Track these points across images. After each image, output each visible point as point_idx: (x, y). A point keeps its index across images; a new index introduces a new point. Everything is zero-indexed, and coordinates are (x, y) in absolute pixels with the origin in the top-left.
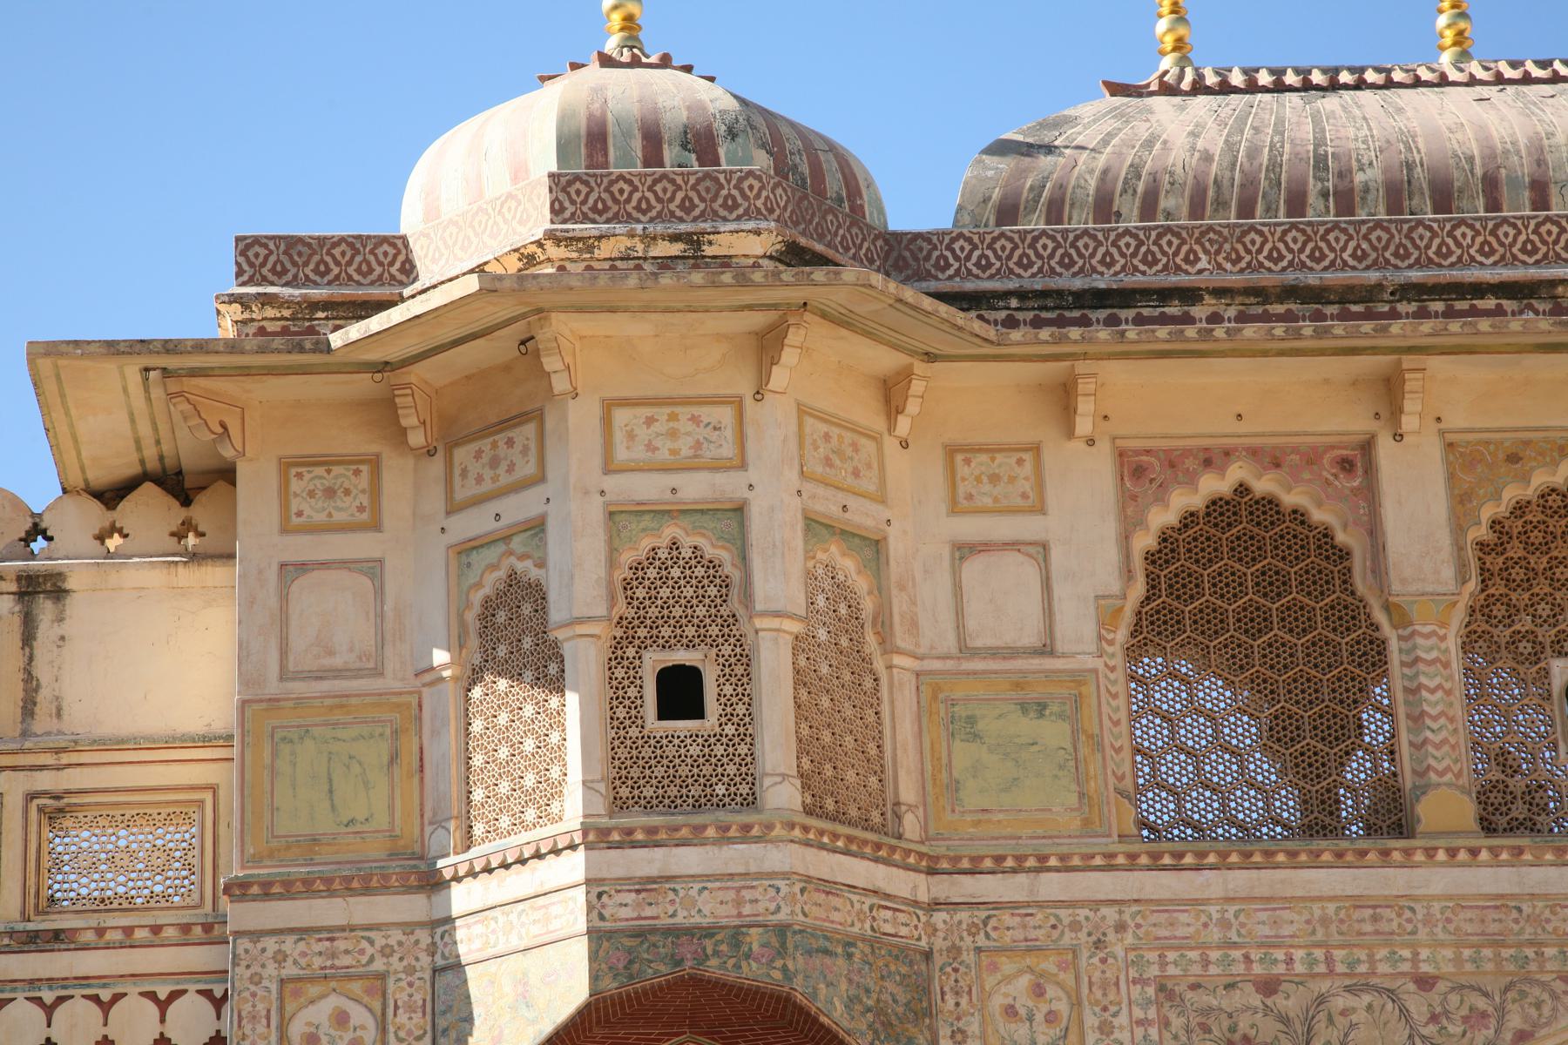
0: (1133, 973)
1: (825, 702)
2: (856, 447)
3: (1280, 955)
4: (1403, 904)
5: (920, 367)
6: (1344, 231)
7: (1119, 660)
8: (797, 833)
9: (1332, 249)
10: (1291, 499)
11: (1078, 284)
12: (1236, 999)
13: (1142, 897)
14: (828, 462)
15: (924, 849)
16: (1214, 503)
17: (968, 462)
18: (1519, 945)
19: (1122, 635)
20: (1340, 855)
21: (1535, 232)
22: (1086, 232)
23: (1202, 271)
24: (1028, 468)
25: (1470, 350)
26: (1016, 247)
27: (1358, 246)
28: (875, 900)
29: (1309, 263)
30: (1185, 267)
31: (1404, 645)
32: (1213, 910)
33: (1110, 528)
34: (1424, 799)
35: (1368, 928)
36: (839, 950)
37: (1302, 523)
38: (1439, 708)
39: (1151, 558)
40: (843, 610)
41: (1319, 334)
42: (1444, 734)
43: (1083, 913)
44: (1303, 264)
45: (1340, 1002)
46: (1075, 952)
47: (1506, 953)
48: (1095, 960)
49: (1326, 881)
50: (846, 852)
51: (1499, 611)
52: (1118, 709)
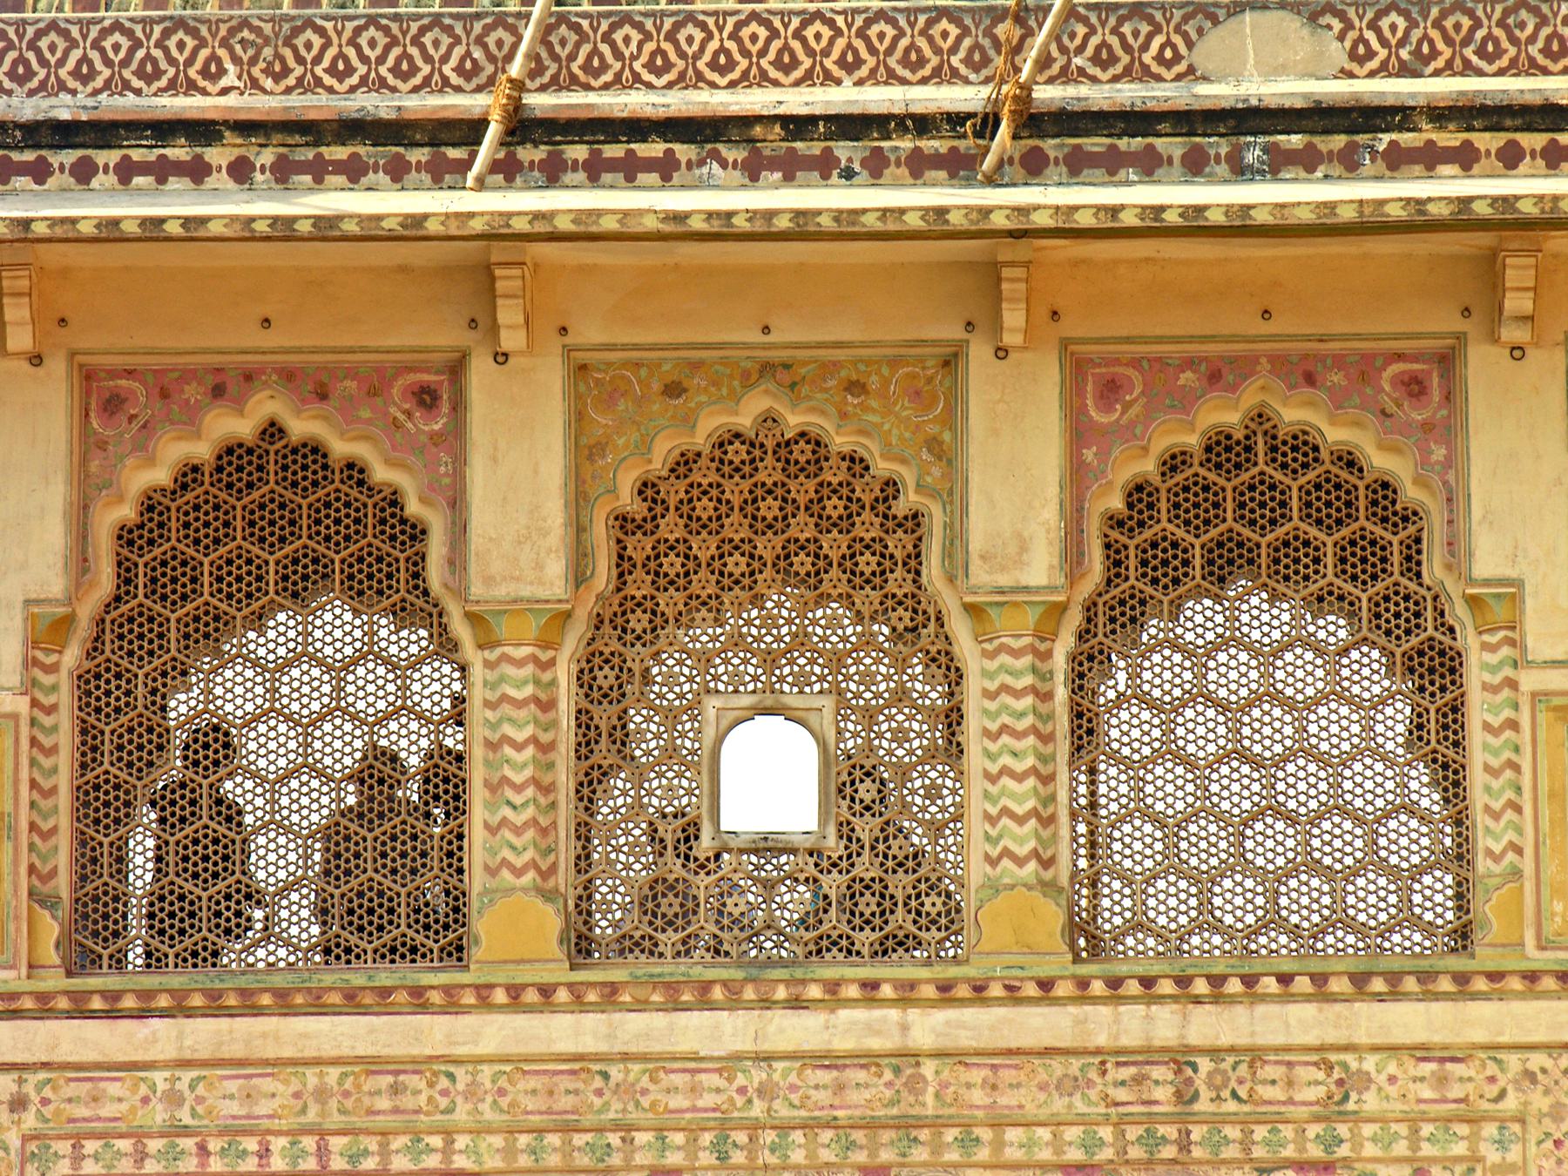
3: (251, 1144)
6: (449, 30)
9: (428, 59)
13: (56, 1058)
16: (230, 451)
18: (600, 1130)
19: (72, 657)
21: (734, 36)
22: (53, 26)
27: (468, 54)
29: (391, 80)
30: (202, 83)
31: (491, 676)
32: (159, 1077)
33: (56, 495)
35: (384, 1103)
37: (361, 483)
39: (126, 536)
44: (383, 83)
47: (579, 1140)
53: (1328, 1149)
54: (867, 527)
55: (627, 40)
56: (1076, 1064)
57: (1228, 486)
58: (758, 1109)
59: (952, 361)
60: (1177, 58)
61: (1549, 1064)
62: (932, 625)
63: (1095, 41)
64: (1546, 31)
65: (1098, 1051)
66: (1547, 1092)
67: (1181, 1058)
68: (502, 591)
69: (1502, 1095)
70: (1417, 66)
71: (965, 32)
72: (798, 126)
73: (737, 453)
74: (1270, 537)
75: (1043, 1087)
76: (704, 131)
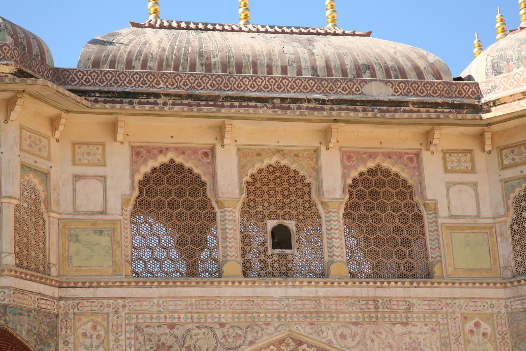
0: (127, 322)
1: (25, 228)
2: (40, 141)
3: (176, 316)
4: (217, 299)
5: (64, 115)
6: (208, 77)
7: (128, 217)
8: (13, 273)
9: (204, 83)
10: (187, 165)
11: (120, 89)
12: (161, 331)
13: (132, 296)
14: (30, 146)
15: (58, 279)
16: (162, 165)
17: (80, 148)
18: (253, 313)
19: (130, 208)
20: (197, 283)
22: (123, 72)
23: (161, 88)
24: (100, 151)
25: (247, 119)
26: (99, 76)
27: (212, 82)
28: (40, 297)
29: (196, 87)
30: (156, 86)
31: (222, 214)
32: (155, 301)
33: (127, 172)
34: (225, 265)
36: (26, 314)
37: (191, 173)
38: (232, 235)
39: (141, 183)
40: (33, 197)
41: (199, 111)
42: (233, 244)
43: (111, 301)
44: (194, 87)
45: (195, 332)
46: (108, 315)
47: (248, 315)
48: (115, 317)
49: (193, 291)
50: (30, 280)
51: (252, 204)
52: (127, 233)
53: (407, 319)
54: (299, 186)
55: (246, 81)
56: (353, 300)
57: (373, 179)
58: (286, 309)
59: (316, 151)
60: (359, 90)
61: (451, 302)
62: (314, 207)
63: (342, 86)
64: (432, 88)
65: (358, 297)
66: (451, 308)
67: (375, 300)
68: (226, 196)
69: (442, 308)
70: (407, 94)
71: (316, 83)
72: (283, 100)
73: (271, 169)
74: (382, 190)
75: (347, 305)
76: (263, 100)
